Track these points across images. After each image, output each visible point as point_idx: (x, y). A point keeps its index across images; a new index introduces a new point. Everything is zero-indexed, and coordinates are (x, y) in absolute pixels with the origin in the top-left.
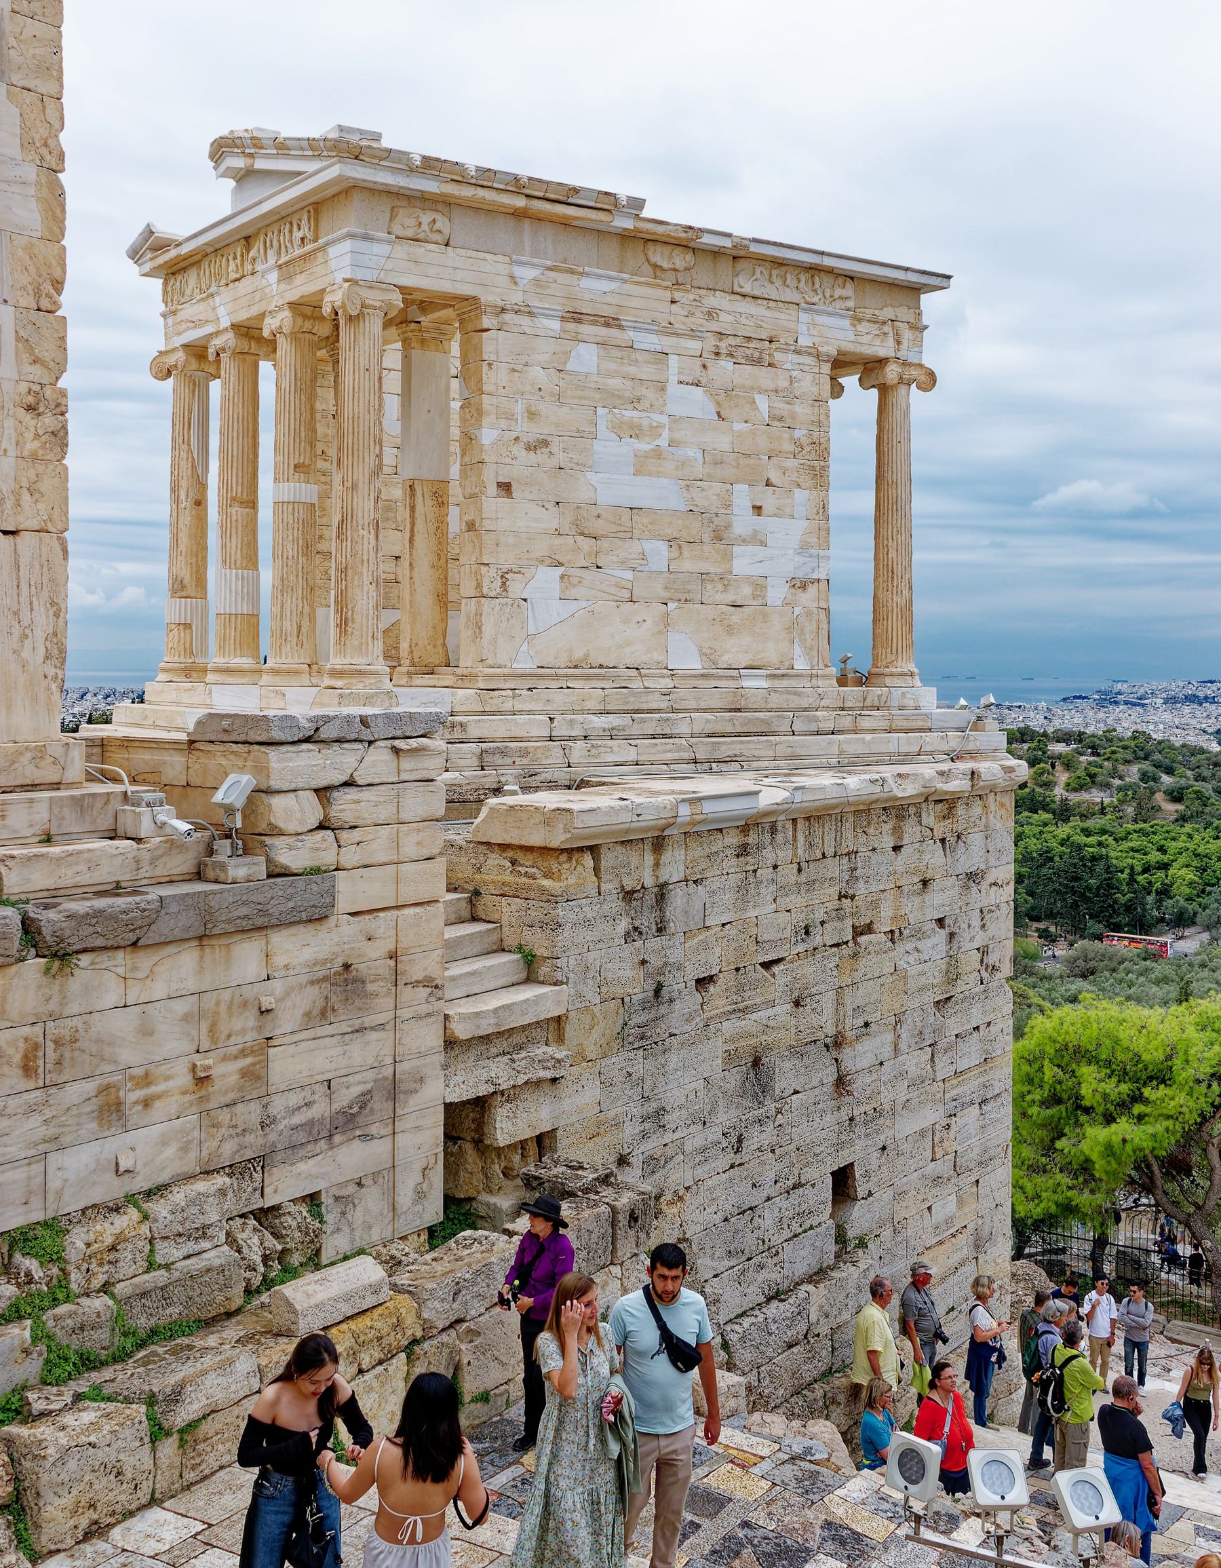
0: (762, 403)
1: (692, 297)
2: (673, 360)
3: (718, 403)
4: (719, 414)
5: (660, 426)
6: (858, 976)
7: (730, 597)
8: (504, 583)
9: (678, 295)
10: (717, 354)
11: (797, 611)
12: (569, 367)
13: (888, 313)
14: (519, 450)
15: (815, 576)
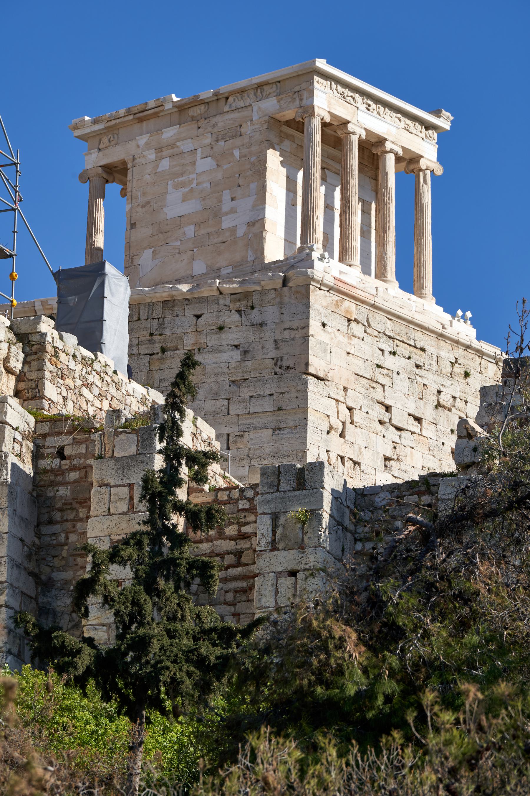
0: (237, 153)
1: (206, 122)
2: (199, 151)
3: (217, 161)
4: (217, 165)
5: (193, 179)
6: (166, 366)
7: (220, 239)
8: (132, 262)
9: (200, 124)
10: (217, 141)
11: (250, 236)
12: (159, 170)
13: (297, 89)
14: (140, 209)
15: (259, 218)
